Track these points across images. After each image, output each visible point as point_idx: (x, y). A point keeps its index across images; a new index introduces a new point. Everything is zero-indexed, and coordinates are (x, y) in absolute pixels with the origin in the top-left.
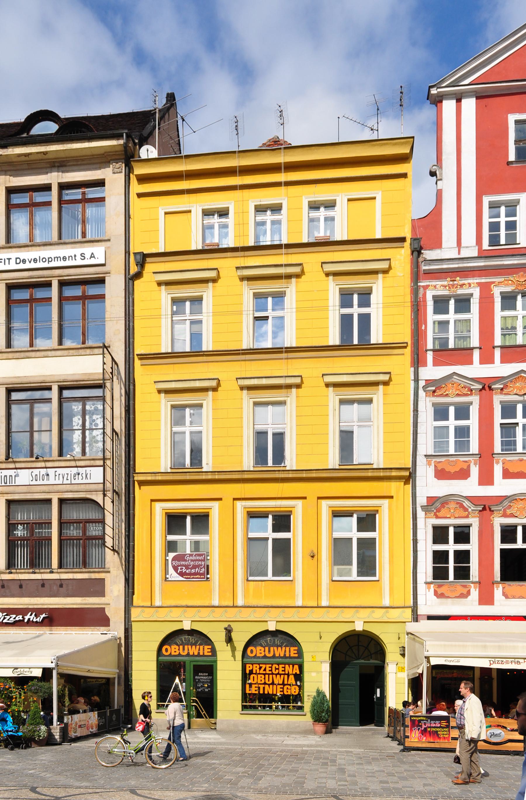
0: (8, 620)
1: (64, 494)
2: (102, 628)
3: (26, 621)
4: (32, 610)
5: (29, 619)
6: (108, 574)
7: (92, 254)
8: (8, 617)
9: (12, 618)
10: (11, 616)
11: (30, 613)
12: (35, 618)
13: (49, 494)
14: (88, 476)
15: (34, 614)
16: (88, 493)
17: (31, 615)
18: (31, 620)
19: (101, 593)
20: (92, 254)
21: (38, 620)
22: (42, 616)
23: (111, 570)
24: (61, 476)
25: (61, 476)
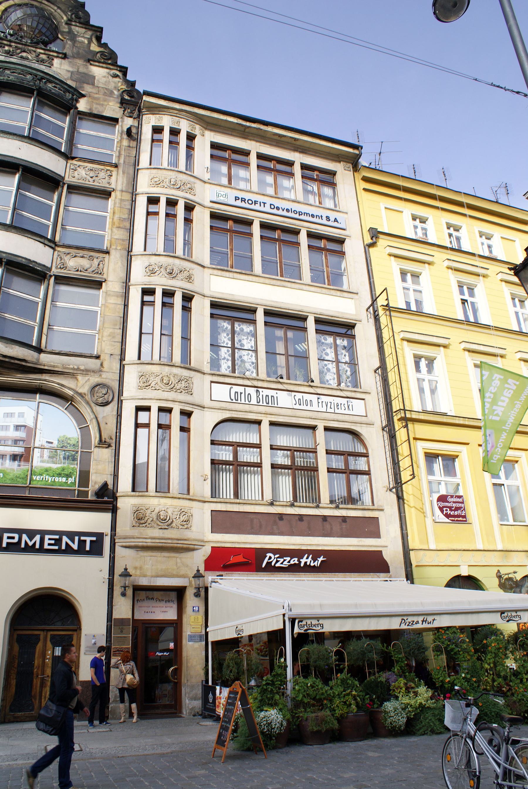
0: (282, 563)
1: (329, 422)
2: (382, 575)
3: (302, 565)
4: (309, 552)
5: (306, 563)
6: (381, 512)
7: (336, 219)
8: (282, 560)
9: (286, 562)
10: (285, 558)
11: (306, 555)
12: (312, 561)
13: (314, 420)
14: (350, 407)
15: (311, 556)
16: (353, 424)
17: (307, 558)
18: (308, 564)
19: (376, 534)
20: (336, 219)
21: (316, 563)
22: (321, 559)
23: (385, 508)
24: (324, 403)
25: (324, 404)
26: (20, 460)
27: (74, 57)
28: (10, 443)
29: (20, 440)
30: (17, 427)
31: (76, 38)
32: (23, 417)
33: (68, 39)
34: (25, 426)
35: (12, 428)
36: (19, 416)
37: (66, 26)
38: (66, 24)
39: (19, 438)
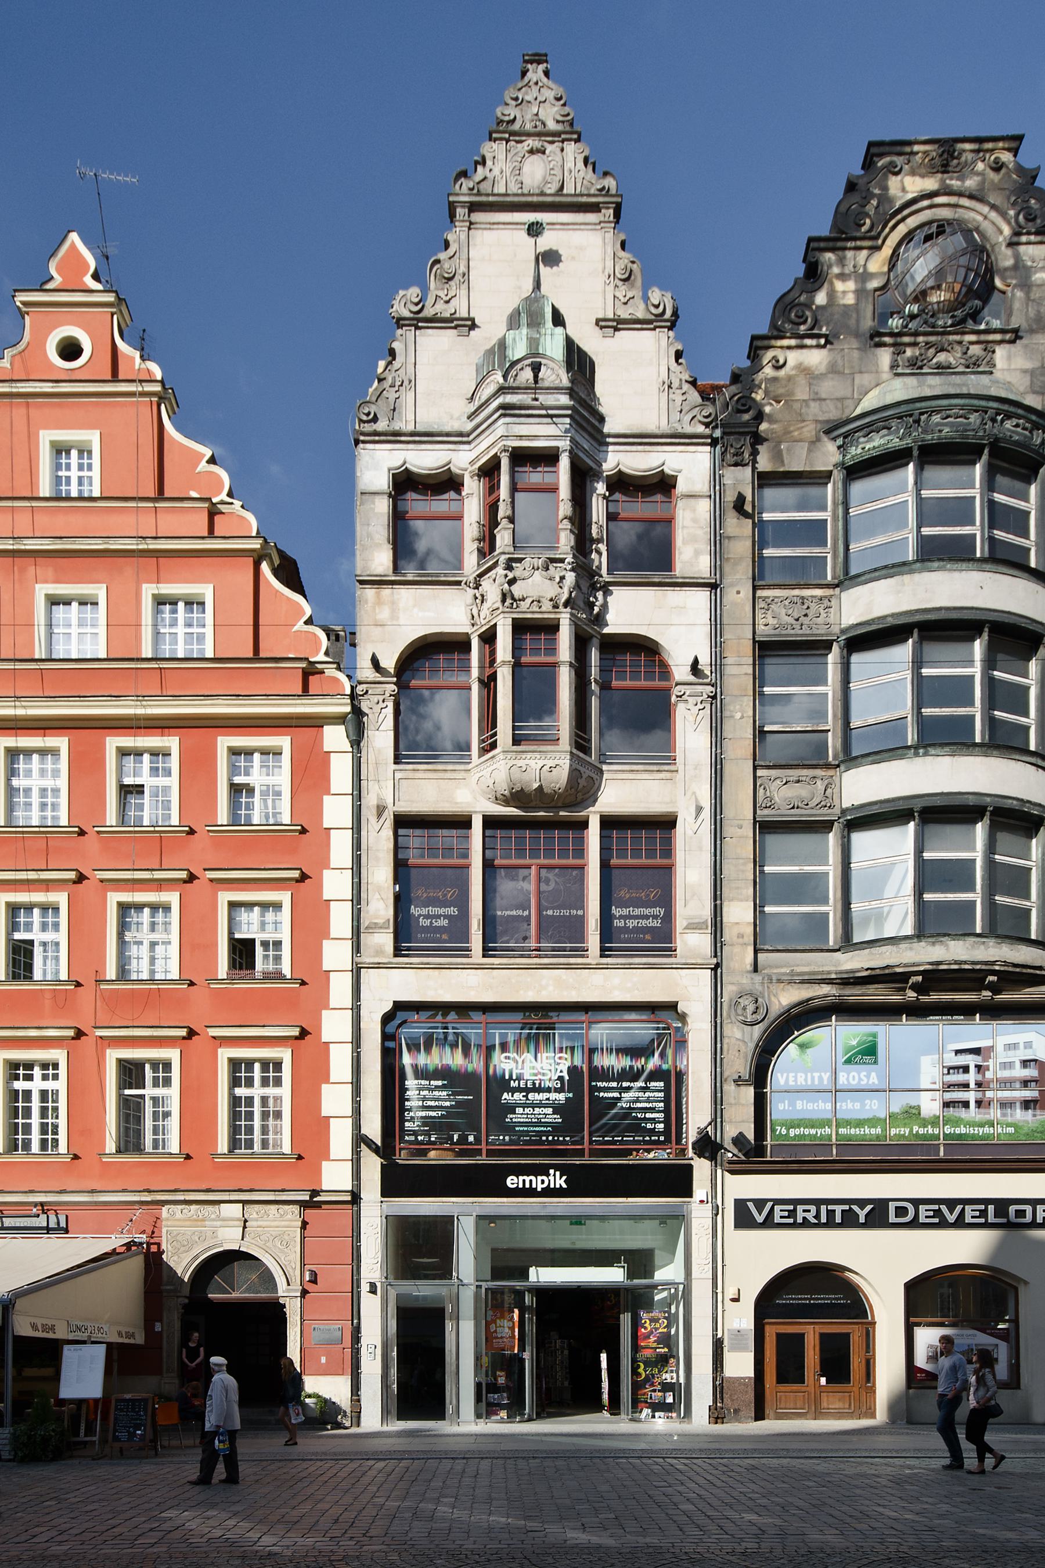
26: (1035, 1109)
27: (1032, 331)
28: (1018, 1085)
29: (1031, 1081)
30: (1025, 1063)
31: (1030, 277)
32: (1031, 1047)
33: (1015, 286)
34: (1036, 1061)
35: (1018, 1065)
36: (1025, 1048)
37: (1009, 252)
38: (1011, 244)
39: (1029, 1078)
